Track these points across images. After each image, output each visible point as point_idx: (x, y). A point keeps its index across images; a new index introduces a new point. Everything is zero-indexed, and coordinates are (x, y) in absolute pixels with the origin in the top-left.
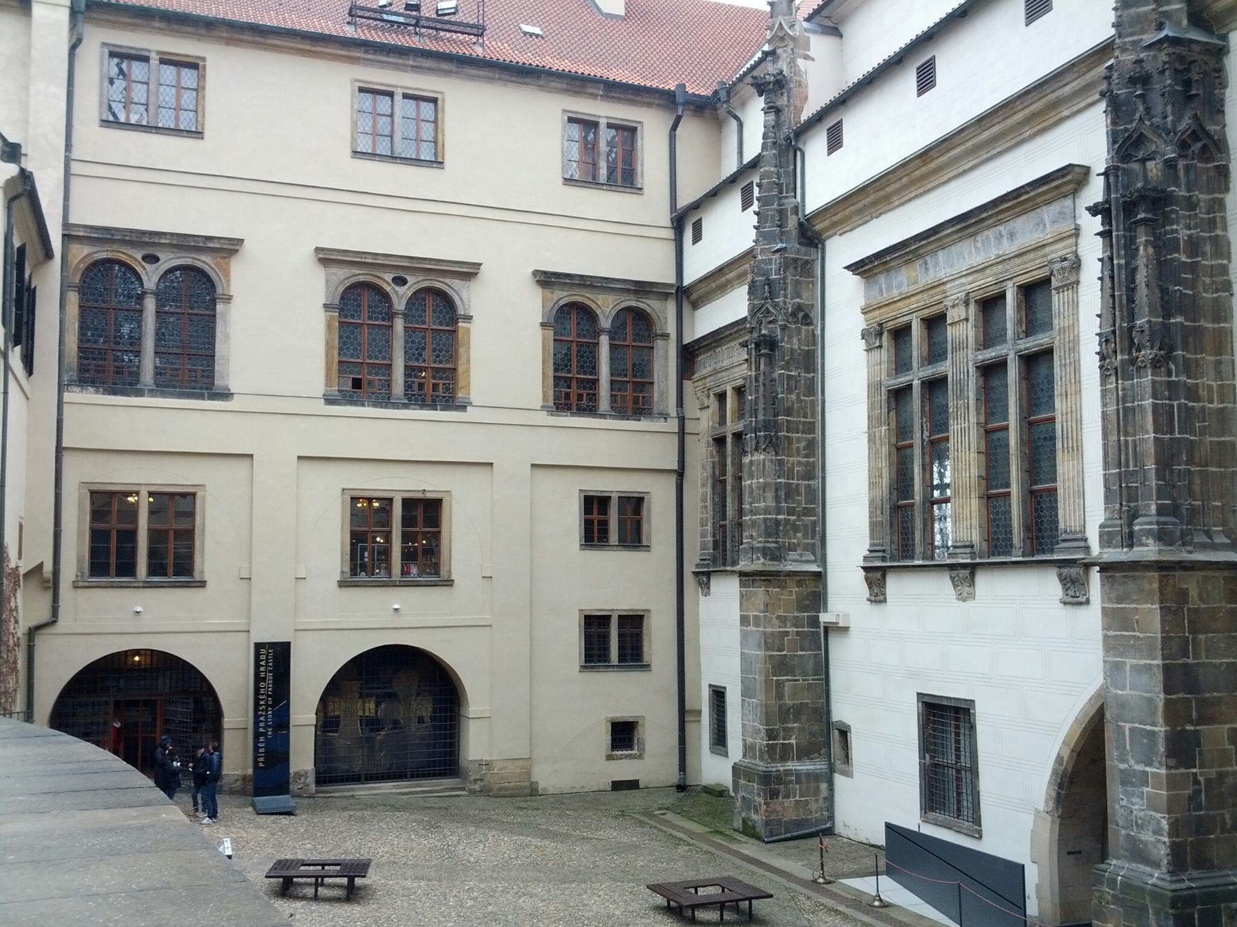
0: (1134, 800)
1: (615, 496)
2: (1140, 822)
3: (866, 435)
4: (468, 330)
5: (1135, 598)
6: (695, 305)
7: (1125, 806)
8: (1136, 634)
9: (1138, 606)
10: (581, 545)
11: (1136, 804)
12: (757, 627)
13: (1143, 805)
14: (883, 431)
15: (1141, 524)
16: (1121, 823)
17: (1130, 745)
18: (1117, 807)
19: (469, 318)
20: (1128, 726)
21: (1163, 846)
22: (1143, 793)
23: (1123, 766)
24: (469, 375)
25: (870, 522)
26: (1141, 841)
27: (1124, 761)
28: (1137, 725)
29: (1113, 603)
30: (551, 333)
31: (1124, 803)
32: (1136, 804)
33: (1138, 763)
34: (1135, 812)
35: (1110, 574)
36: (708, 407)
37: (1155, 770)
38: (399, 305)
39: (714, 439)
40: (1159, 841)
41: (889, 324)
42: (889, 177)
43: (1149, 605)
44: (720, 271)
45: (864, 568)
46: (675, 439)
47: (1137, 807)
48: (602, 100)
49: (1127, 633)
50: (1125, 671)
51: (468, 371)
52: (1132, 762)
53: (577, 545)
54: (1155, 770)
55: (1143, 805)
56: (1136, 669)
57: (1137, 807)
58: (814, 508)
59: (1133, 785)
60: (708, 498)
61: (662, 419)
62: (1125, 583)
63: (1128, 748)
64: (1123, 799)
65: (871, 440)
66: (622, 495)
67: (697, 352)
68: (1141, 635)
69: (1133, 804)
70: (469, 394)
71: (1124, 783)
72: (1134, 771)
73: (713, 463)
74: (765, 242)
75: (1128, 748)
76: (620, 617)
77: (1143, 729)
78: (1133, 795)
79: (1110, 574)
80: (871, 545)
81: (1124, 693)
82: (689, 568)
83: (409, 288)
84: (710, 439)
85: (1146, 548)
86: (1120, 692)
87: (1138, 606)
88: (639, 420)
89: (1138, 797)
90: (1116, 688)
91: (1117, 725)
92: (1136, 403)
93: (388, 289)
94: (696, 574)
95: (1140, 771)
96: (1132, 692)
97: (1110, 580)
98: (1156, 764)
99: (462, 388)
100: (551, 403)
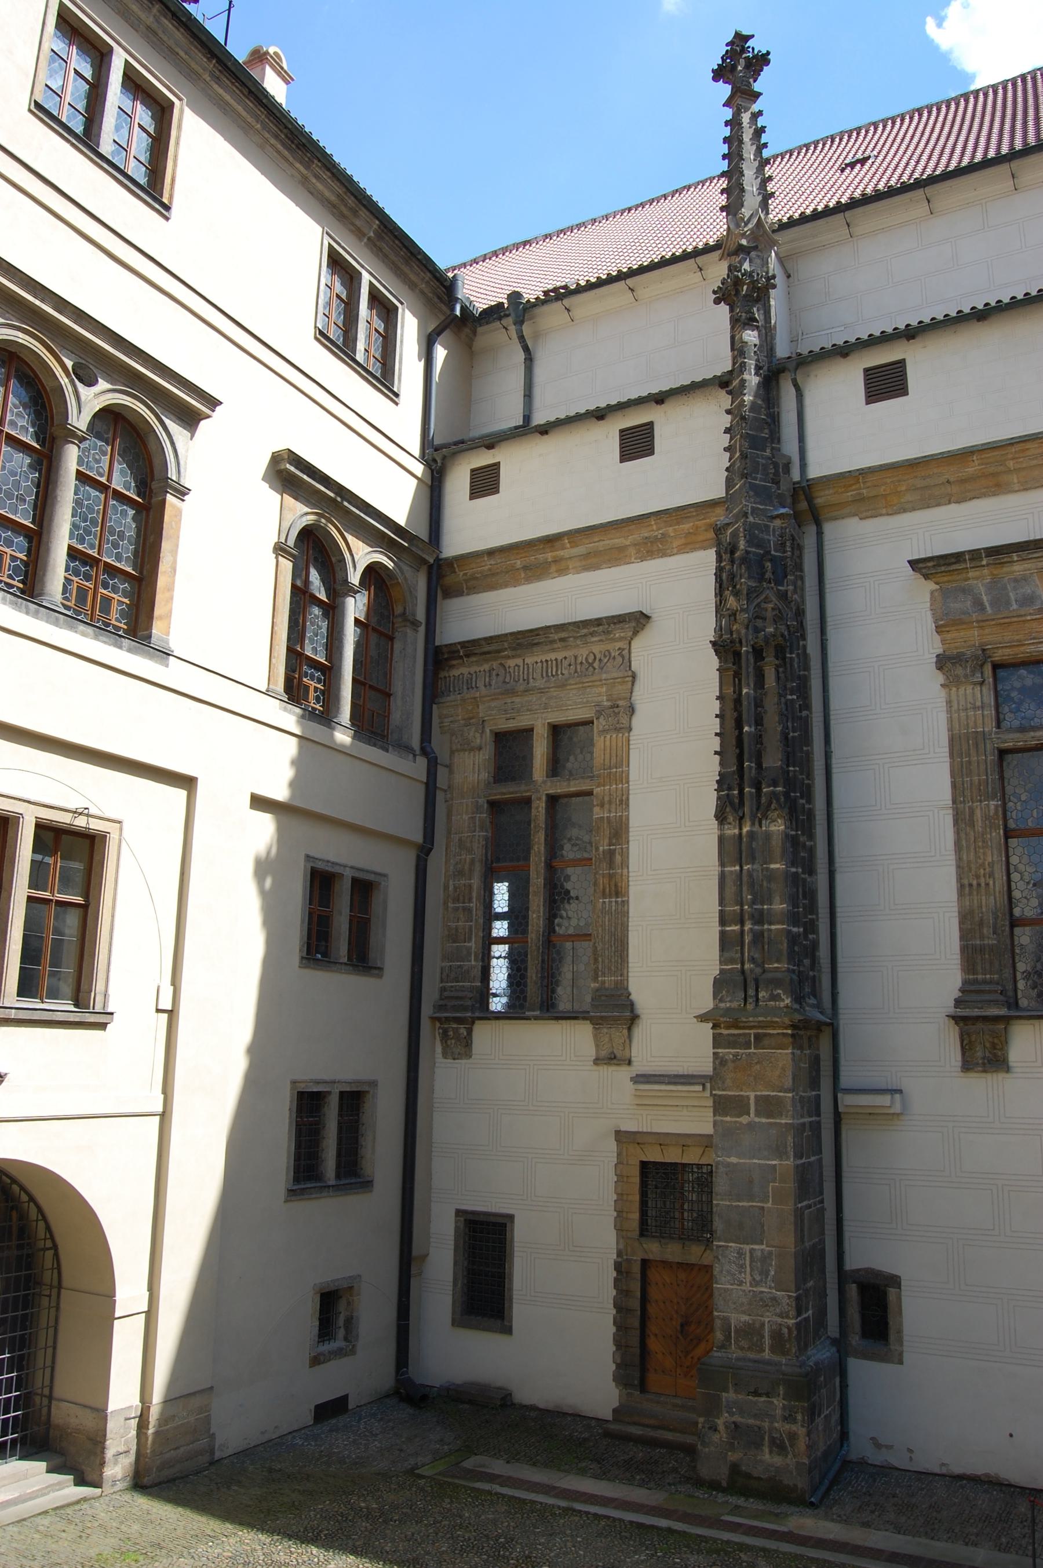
1: (348, 874)
3: (951, 811)
4: (179, 513)
6: (450, 593)
10: (302, 958)
12: (770, 1116)
14: (992, 807)
19: (182, 493)
24: (172, 598)
25: (964, 949)
30: (287, 565)
36: (480, 748)
38: (80, 420)
39: (488, 802)
41: (1000, 652)
42: (1028, 445)
44: (551, 541)
45: (956, 1019)
46: (420, 792)
48: (366, 245)
51: (170, 588)
53: (296, 959)
58: (813, 919)
60: (474, 894)
61: (411, 756)
65: (962, 820)
66: (357, 875)
67: (454, 662)
70: (168, 634)
73: (486, 839)
74: (758, 500)
76: (342, 1094)
80: (965, 982)
82: (427, 1010)
83: (97, 395)
84: (482, 801)
88: (387, 751)
93: (64, 381)
94: (433, 1019)
99: (160, 618)
100: (280, 686)
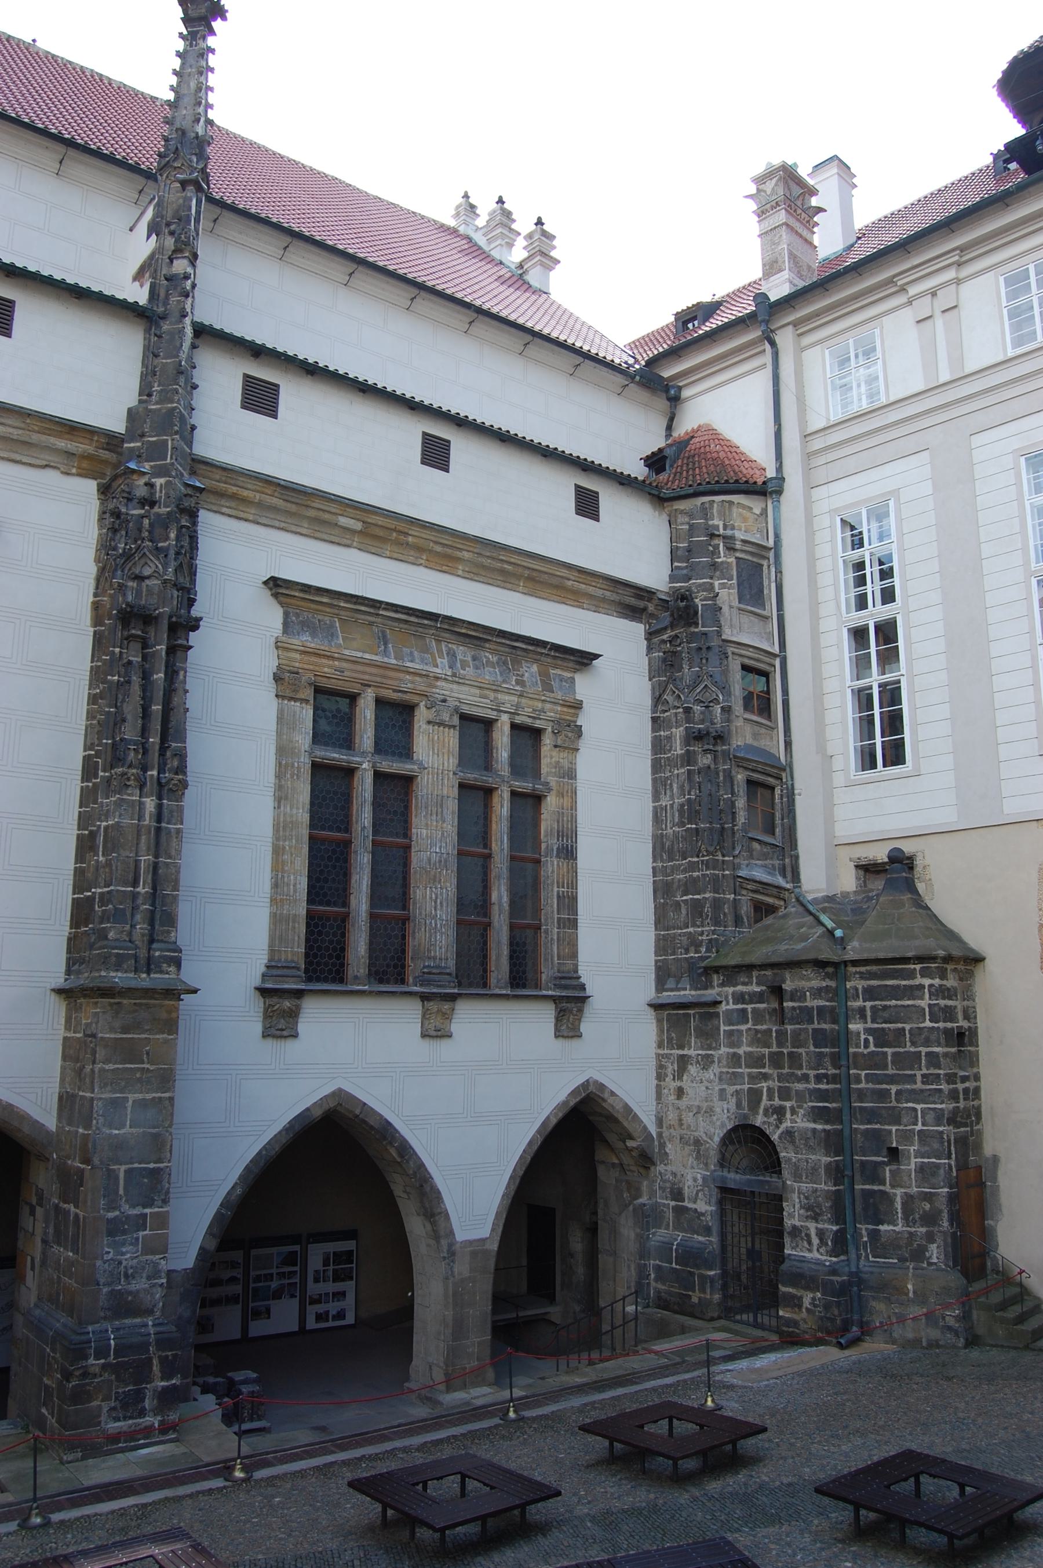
0: (124, 1250)
2: (130, 1271)
5: (146, 1027)
7: (112, 1259)
8: (146, 1066)
9: (151, 1037)
11: (127, 1252)
13: (137, 1251)
15: (161, 950)
16: (102, 1281)
17: (125, 1189)
18: (99, 1263)
20: (123, 1168)
21: (159, 1289)
22: (137, 1239)
23: (111, 1215)
26: (130, 1293)
27: (111, 1208)
28: (136, 1165)
29: (116, 1032)
31: (111, 1255)
32: (127, 1252)
33: (133, 1206)
34: (124, 1263)
35: (116, 1001)
37: (156, 1210)
40: (154, 1285)
43: (165, 1036)
47: (128, 1255)
49: (132, 1066)
50: (126, 1108)
52: (125, 1207)
54: (156, 1210)
55: (137, 1251)
56: (142, 1104)
57: (128, 1255)
59: (124, 1232)
62: (135, 1011)
63: (121, 1192)
64: (108, 1253)
68: (152, 1068)
69: (123, 1254)
71: (110, 1233)
72: (128, 1217)
75: (121, 1192)
77: (145, 1169)
78: (123, 1244)
79: (116, 1001)
81: (122, 1131)
85: (167, 976)
86: (117, 1132)
87: (151, 1037)
89: (131, 1244)
90: (111, 1127)
91: (108, 1170)
92: (163, 825)
95: (137, 1215)
96: (134, 1130)
97: (115, 1007)
98: (160, 1203)
